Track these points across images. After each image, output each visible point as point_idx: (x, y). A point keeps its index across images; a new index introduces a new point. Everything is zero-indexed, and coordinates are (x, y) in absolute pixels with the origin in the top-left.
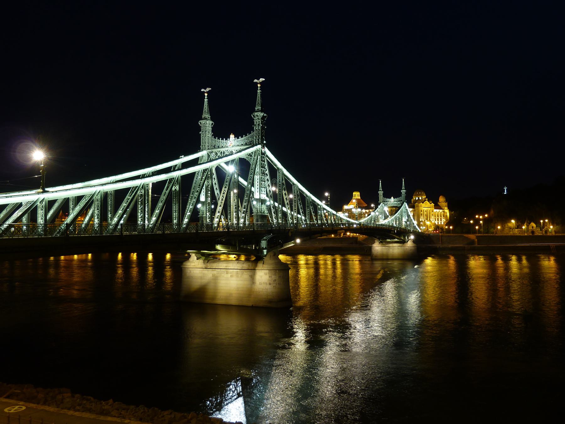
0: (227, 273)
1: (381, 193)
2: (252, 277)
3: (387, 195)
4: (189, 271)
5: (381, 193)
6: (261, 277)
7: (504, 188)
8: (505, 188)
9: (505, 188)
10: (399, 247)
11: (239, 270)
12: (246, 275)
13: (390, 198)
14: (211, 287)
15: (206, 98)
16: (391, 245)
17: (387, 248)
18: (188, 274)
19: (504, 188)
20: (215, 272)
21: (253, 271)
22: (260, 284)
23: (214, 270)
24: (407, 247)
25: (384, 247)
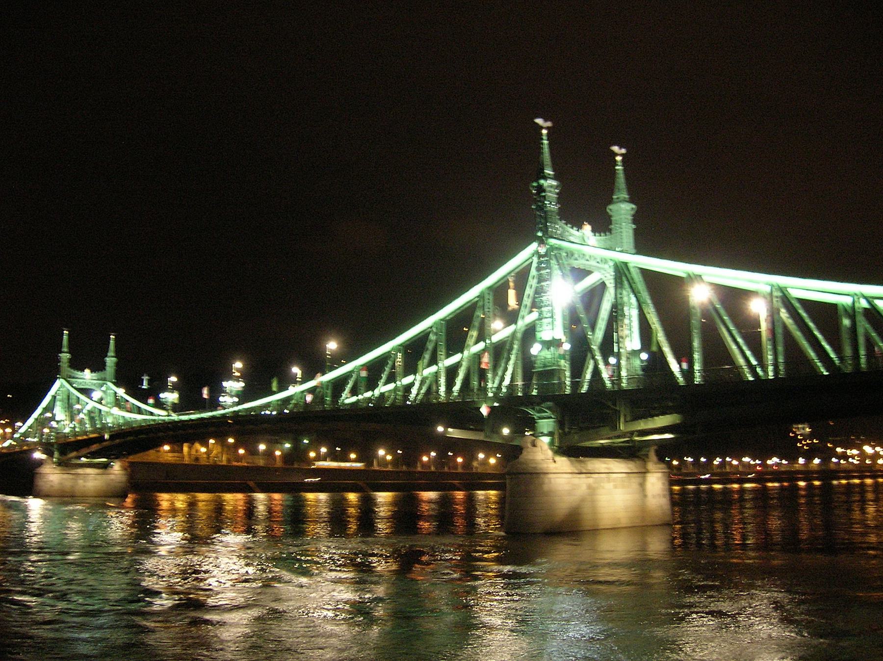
0: (609, 481)
1: (65, 356)
2: (642, 485)
3: (78, 364)
4: (546, 481)
5: (65, 356)
6: (653, 484)
7: (143, 377)
8: (145, 378)
9: (145, 378)
10: (98, 477)
11: (624, 475)
12: (635, 480)
13: (82, 370)
14: (586, 510)
15: (545, 137)
16: (80, 471)
17: (71, 476)
18: (546, 487)
19: (143, 377)
20: (590, 480)
21: (642, 475)
22: (654, 496)
23: (589, 475)
24: (112, 477)
25: (65, 476)
